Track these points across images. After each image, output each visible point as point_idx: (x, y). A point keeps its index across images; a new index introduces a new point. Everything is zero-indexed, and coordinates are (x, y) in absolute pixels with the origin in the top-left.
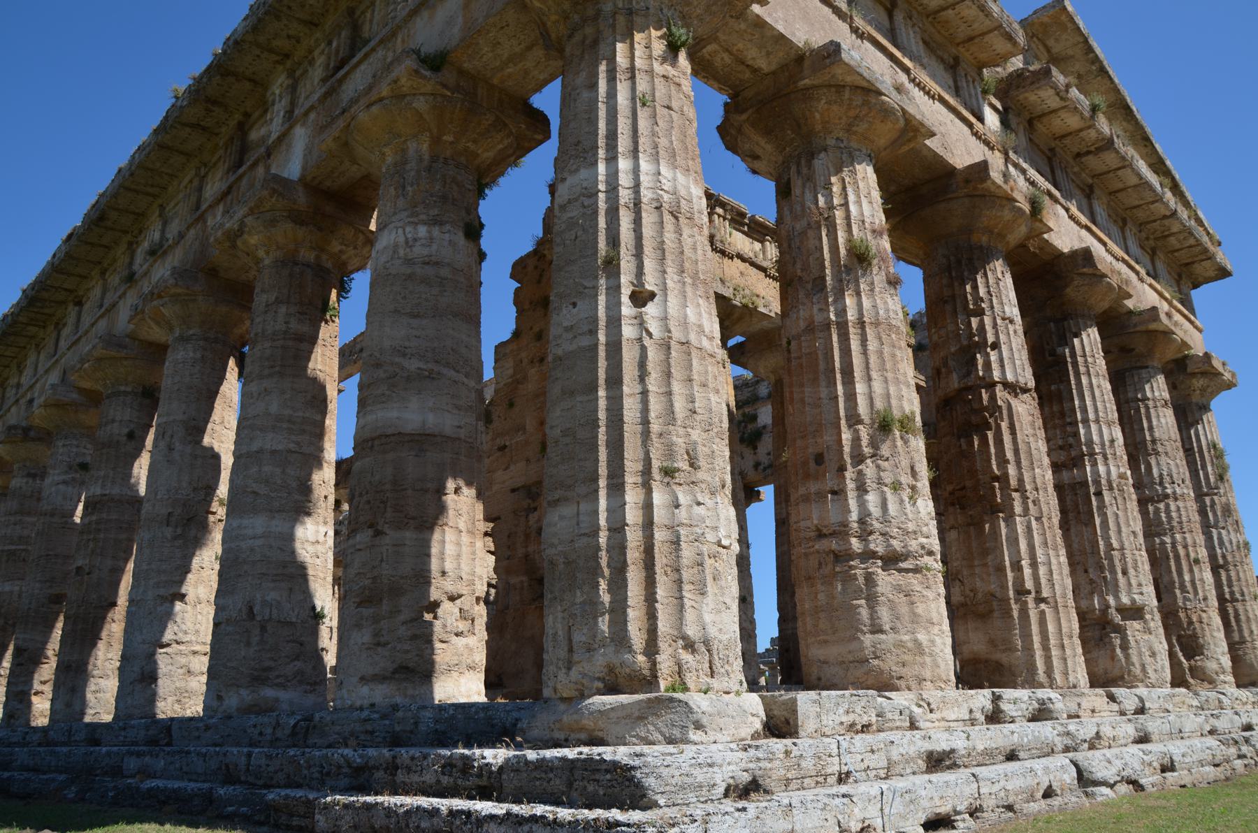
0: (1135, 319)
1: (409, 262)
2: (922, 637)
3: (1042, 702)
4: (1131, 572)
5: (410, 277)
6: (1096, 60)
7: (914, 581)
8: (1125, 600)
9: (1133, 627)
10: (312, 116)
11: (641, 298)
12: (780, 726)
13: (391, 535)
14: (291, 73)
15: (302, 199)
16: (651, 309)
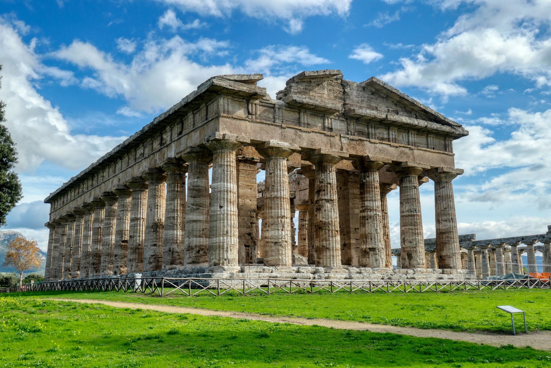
0: (403, 164)
1: (193, 186)
2: (280, 257)
3: (316, 270)
4: (373, 239)
5: (194, 189)
6: (389, 90)
8: (371, 246)
9: (371, 253)
10: (175, 142)
11: (221, 207)
12: (242, 271)
13: (191, 239)
14: (171, 127)
15: (174, 161)
16: (222, 209)
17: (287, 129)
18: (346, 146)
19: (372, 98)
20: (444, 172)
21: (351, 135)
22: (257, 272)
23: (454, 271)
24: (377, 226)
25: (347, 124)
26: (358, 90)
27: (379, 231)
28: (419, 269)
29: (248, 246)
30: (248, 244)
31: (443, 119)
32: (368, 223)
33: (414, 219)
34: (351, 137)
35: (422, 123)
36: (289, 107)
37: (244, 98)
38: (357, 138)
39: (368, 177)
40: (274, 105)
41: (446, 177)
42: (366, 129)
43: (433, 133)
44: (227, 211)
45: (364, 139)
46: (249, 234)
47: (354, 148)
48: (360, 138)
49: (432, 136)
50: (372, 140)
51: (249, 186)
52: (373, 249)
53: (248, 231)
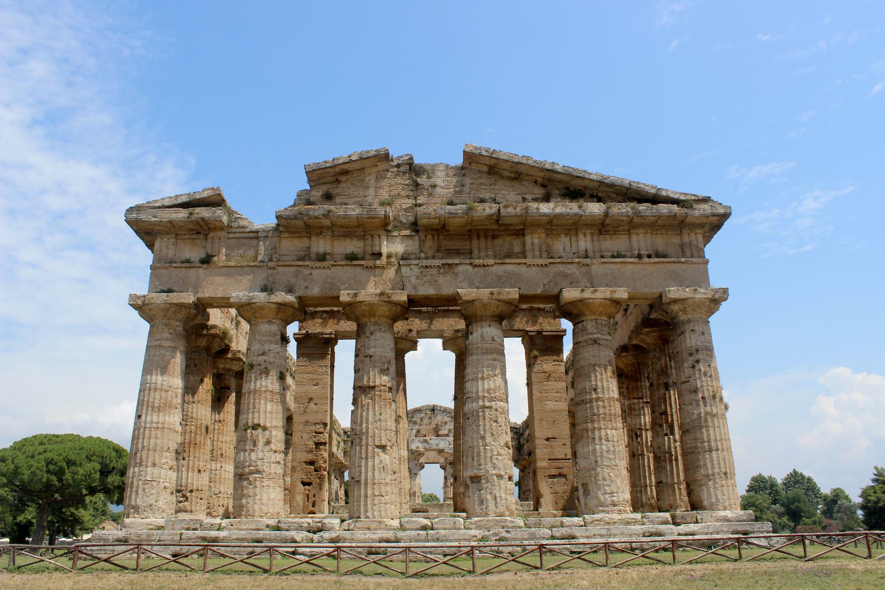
7: (245, 483)
17: (281, 269)
18: (413, 280)
19: (481, 184)
20: (675, 301)
21: (427, 258)
22: (188, 529)
23: (700, 514)
24: (485, 430)
25: (419, 239)
26: (447, 175)
27: (489, 439)
28: (596, 516)
29: (309, 484)
30: (307, 480)
31: (653, 191)
32: (469, 425)
33: (592, 407)
34: (425, 263)
35: (595, 208)
36: (289, 232)
37: (198, 233)
38: (437, 262)
39: (472, 333)
40: (257, 232)
41: (684, 311)
42: (468, 243)
43: (642, 225)
44: (146, 422)
45: (457, 261)
46: (312, 463)
47: (434, 283)
48: (443, 261)
49: (641, 231)
50: (477, 262)
51: (313, 380)
52: (476, 479)
53: (310, 457)
